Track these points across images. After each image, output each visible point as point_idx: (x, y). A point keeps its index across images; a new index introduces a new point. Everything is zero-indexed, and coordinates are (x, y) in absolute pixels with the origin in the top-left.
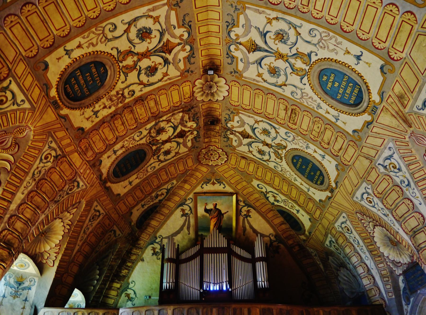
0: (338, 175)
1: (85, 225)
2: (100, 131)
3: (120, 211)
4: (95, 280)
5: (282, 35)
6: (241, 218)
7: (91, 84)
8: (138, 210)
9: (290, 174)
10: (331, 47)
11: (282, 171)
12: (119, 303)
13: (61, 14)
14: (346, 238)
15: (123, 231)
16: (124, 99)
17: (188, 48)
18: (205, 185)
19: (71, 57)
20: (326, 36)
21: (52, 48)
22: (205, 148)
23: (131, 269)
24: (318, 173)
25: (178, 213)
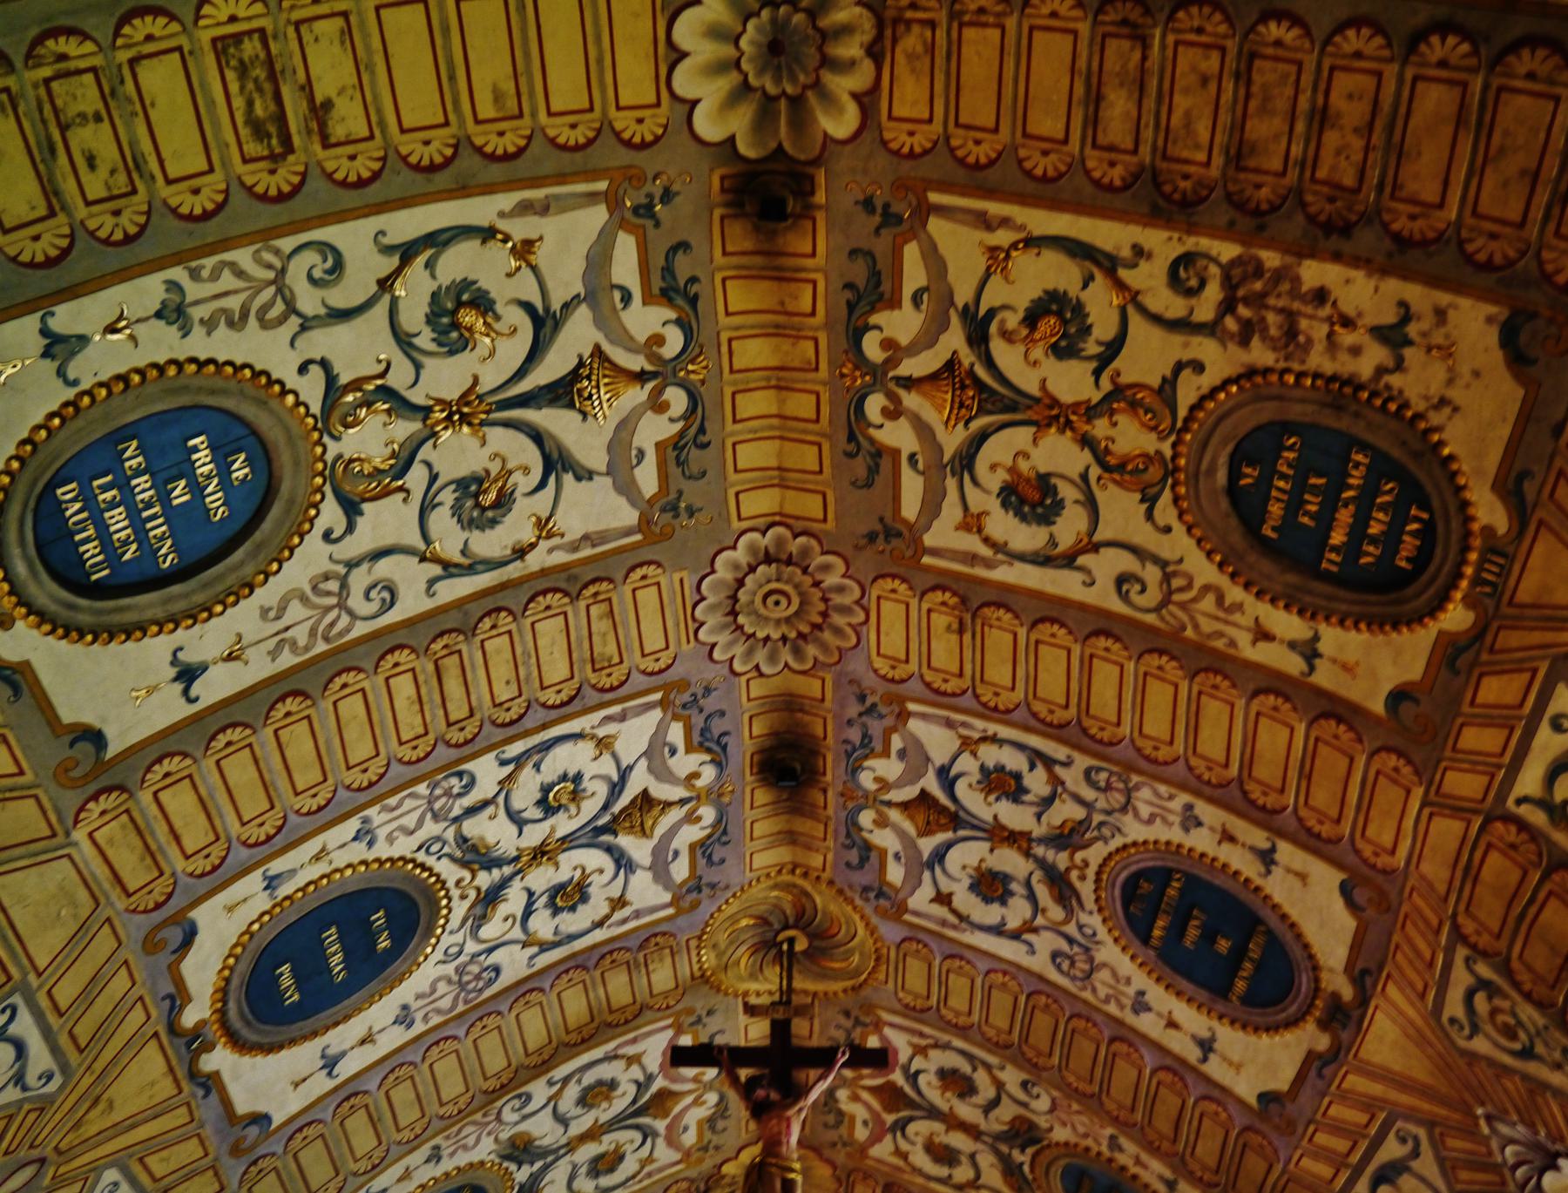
5: (484, 509)
7: (1320, 476)
10: (296, 611)
13: (1250, 740)
16: (1237, 272)
17: (872, 347)
19: (1309, 634)
20: (332, 624)
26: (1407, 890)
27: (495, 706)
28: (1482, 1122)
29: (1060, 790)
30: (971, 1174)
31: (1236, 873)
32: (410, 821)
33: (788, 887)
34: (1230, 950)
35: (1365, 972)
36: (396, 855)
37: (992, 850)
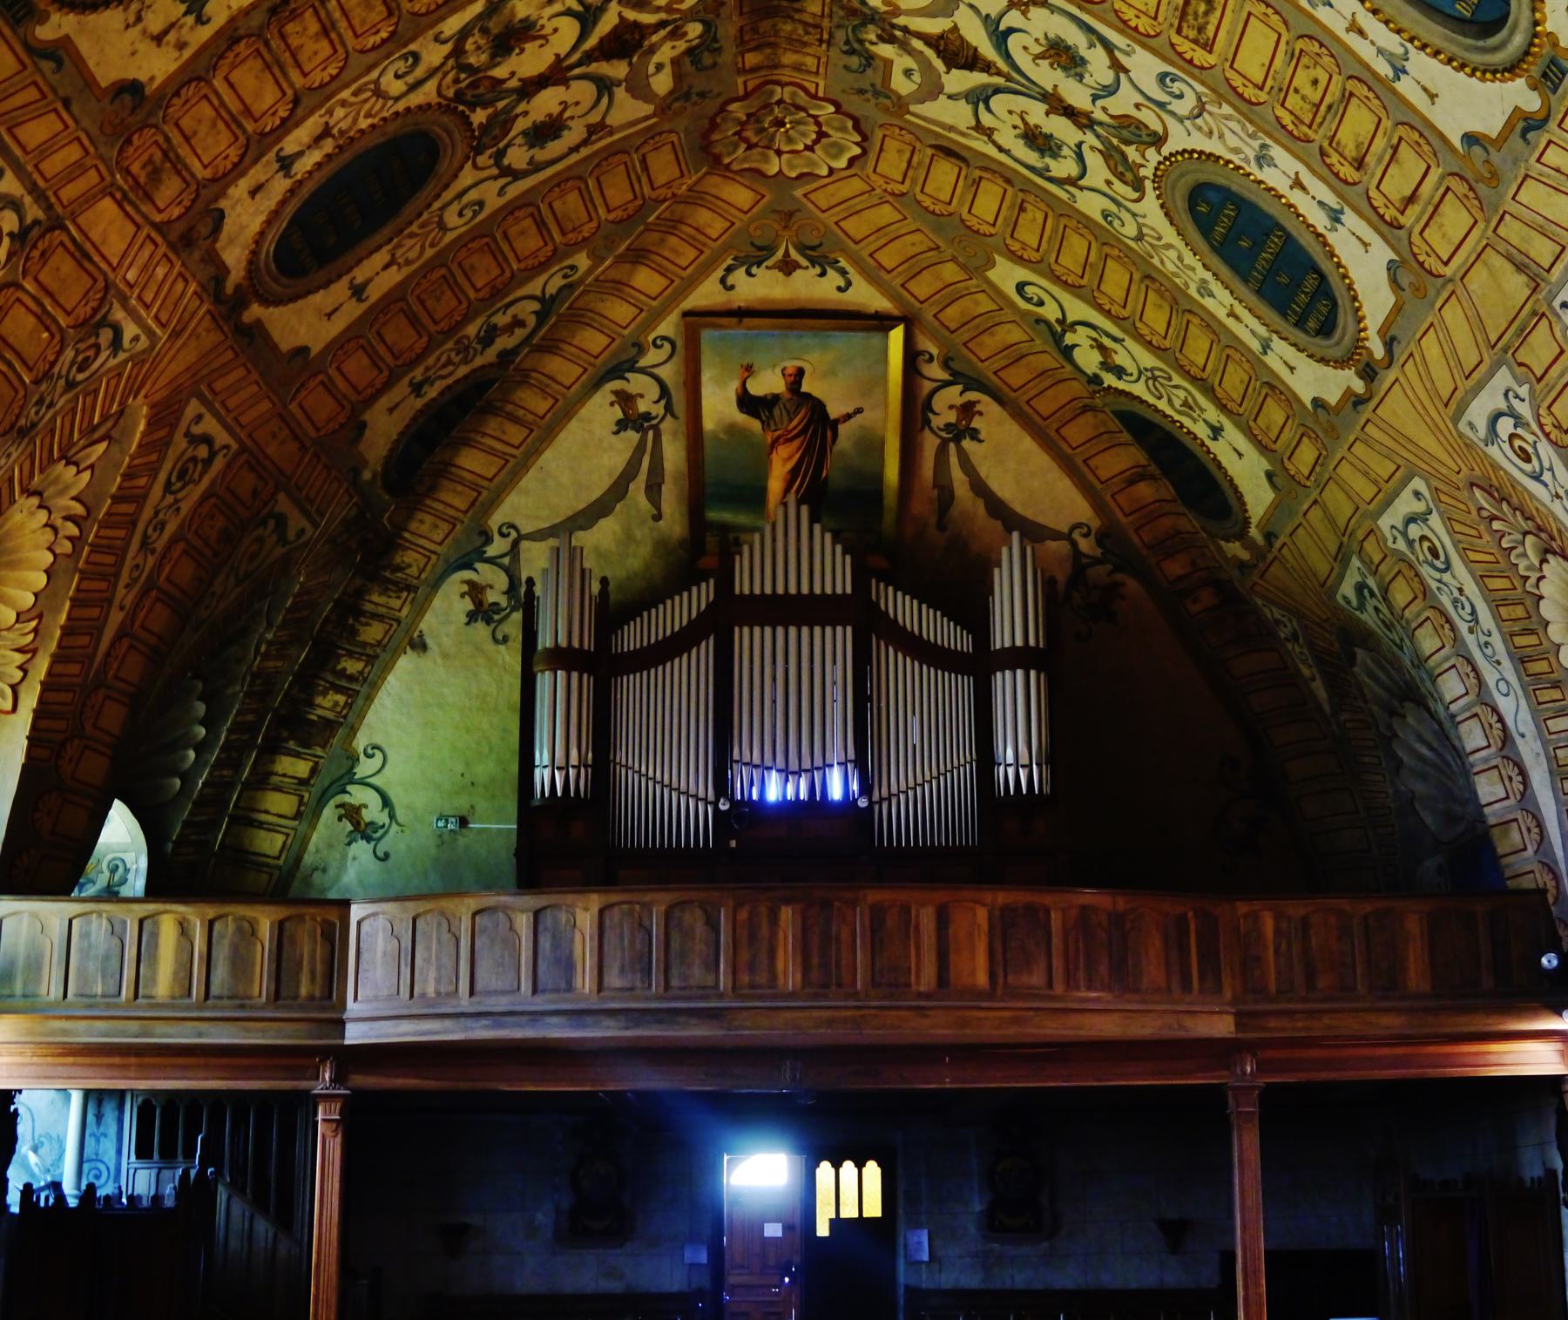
0: (1398, 309)
1: (148, 512)
2: (218, 83)
3: (307, 425)
4: (186, 747)
6: (930, 443)
8: (391, 410)
9: (1180, 258)
11: (1140, 237)
12: (311, 847)
14: (1426, 591)
15: (322, 515)
18: (739, 276)
22: (747, 95)
23: (364, 690)
24: (1310, 283)
25: (600, 411)
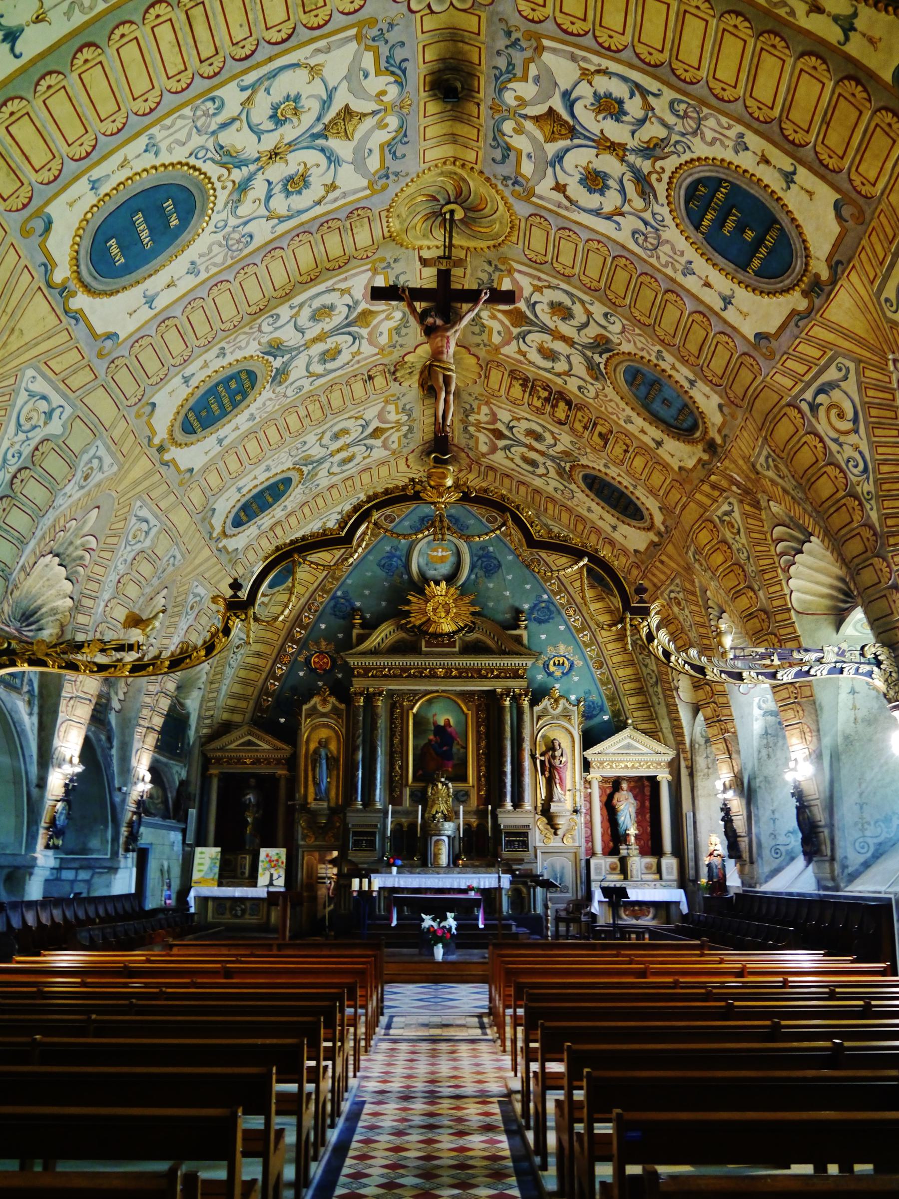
13: (793, 90)
21: (861, 75)
26: (878, 211)
27: (233, 44)
28: (890, 363)
29: (650, 114)
30: (567, 368)
31: (767, 186)
32: (182, 136)
33: (450, 174)
34: (753, 239)
35: (839, 262)
36: (175, 162)
37: (597, 156)
